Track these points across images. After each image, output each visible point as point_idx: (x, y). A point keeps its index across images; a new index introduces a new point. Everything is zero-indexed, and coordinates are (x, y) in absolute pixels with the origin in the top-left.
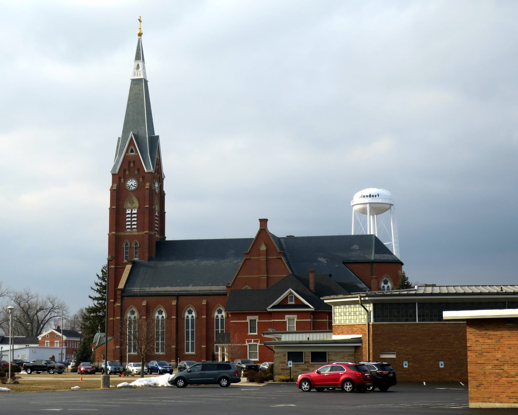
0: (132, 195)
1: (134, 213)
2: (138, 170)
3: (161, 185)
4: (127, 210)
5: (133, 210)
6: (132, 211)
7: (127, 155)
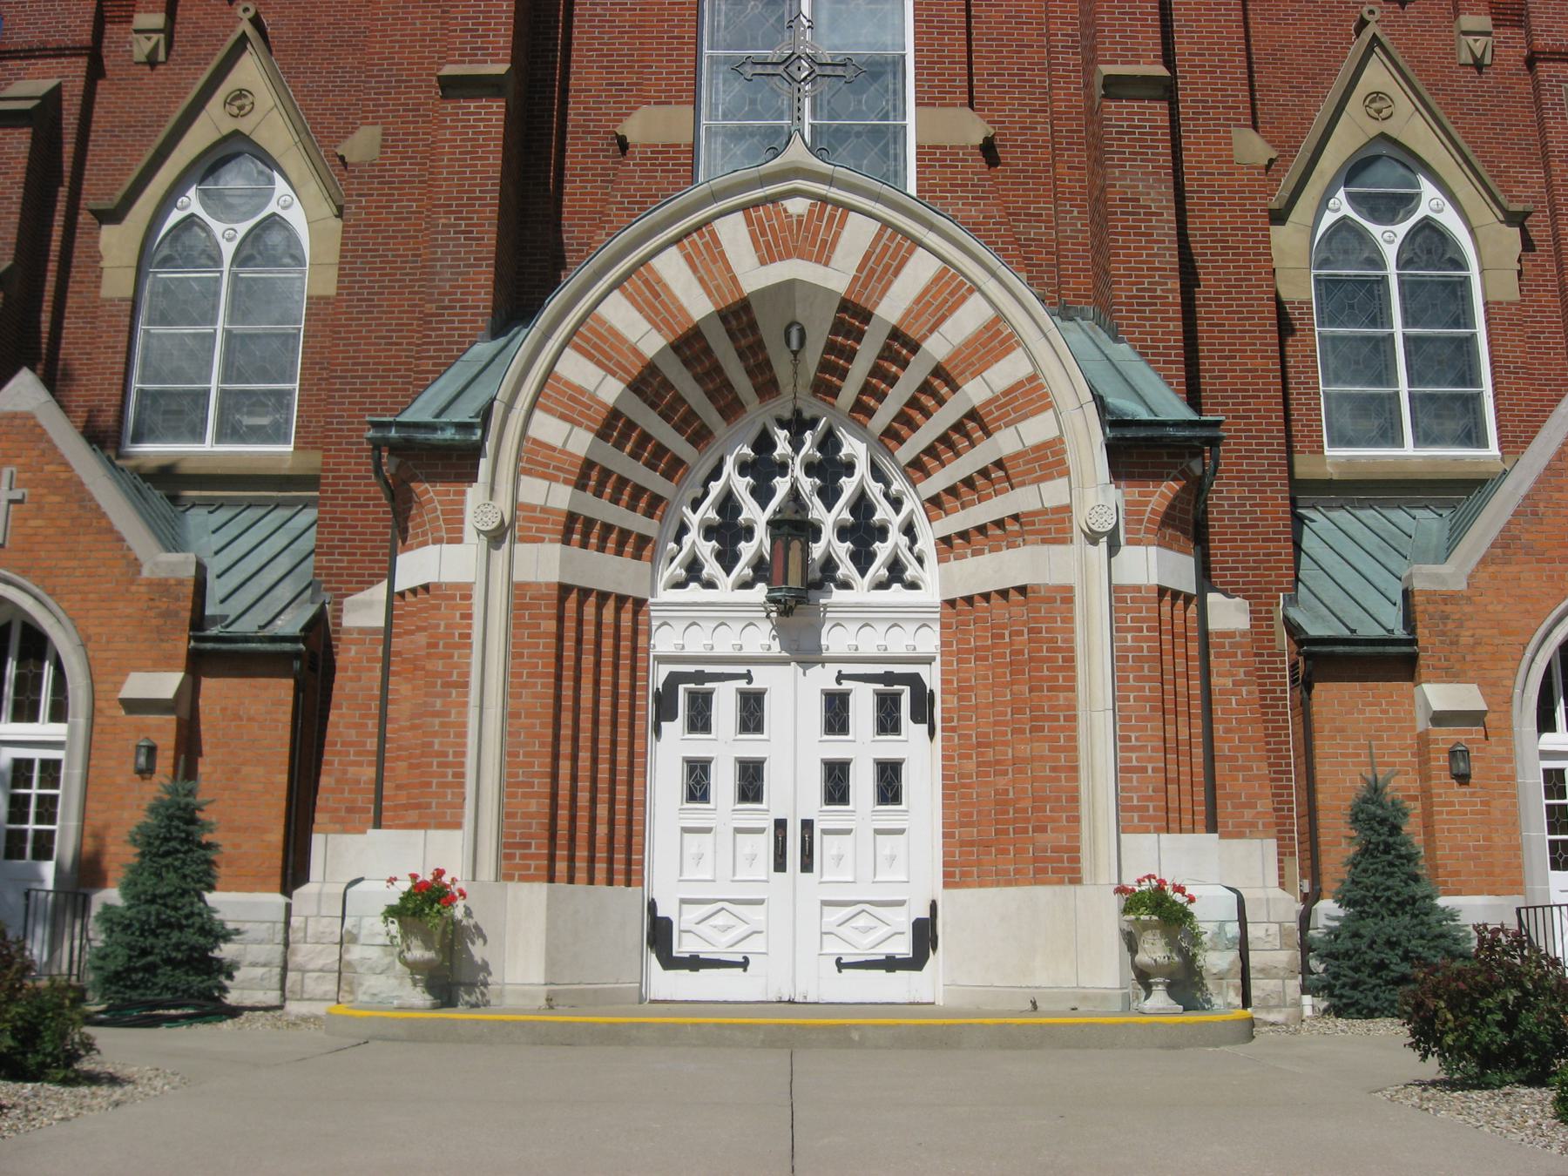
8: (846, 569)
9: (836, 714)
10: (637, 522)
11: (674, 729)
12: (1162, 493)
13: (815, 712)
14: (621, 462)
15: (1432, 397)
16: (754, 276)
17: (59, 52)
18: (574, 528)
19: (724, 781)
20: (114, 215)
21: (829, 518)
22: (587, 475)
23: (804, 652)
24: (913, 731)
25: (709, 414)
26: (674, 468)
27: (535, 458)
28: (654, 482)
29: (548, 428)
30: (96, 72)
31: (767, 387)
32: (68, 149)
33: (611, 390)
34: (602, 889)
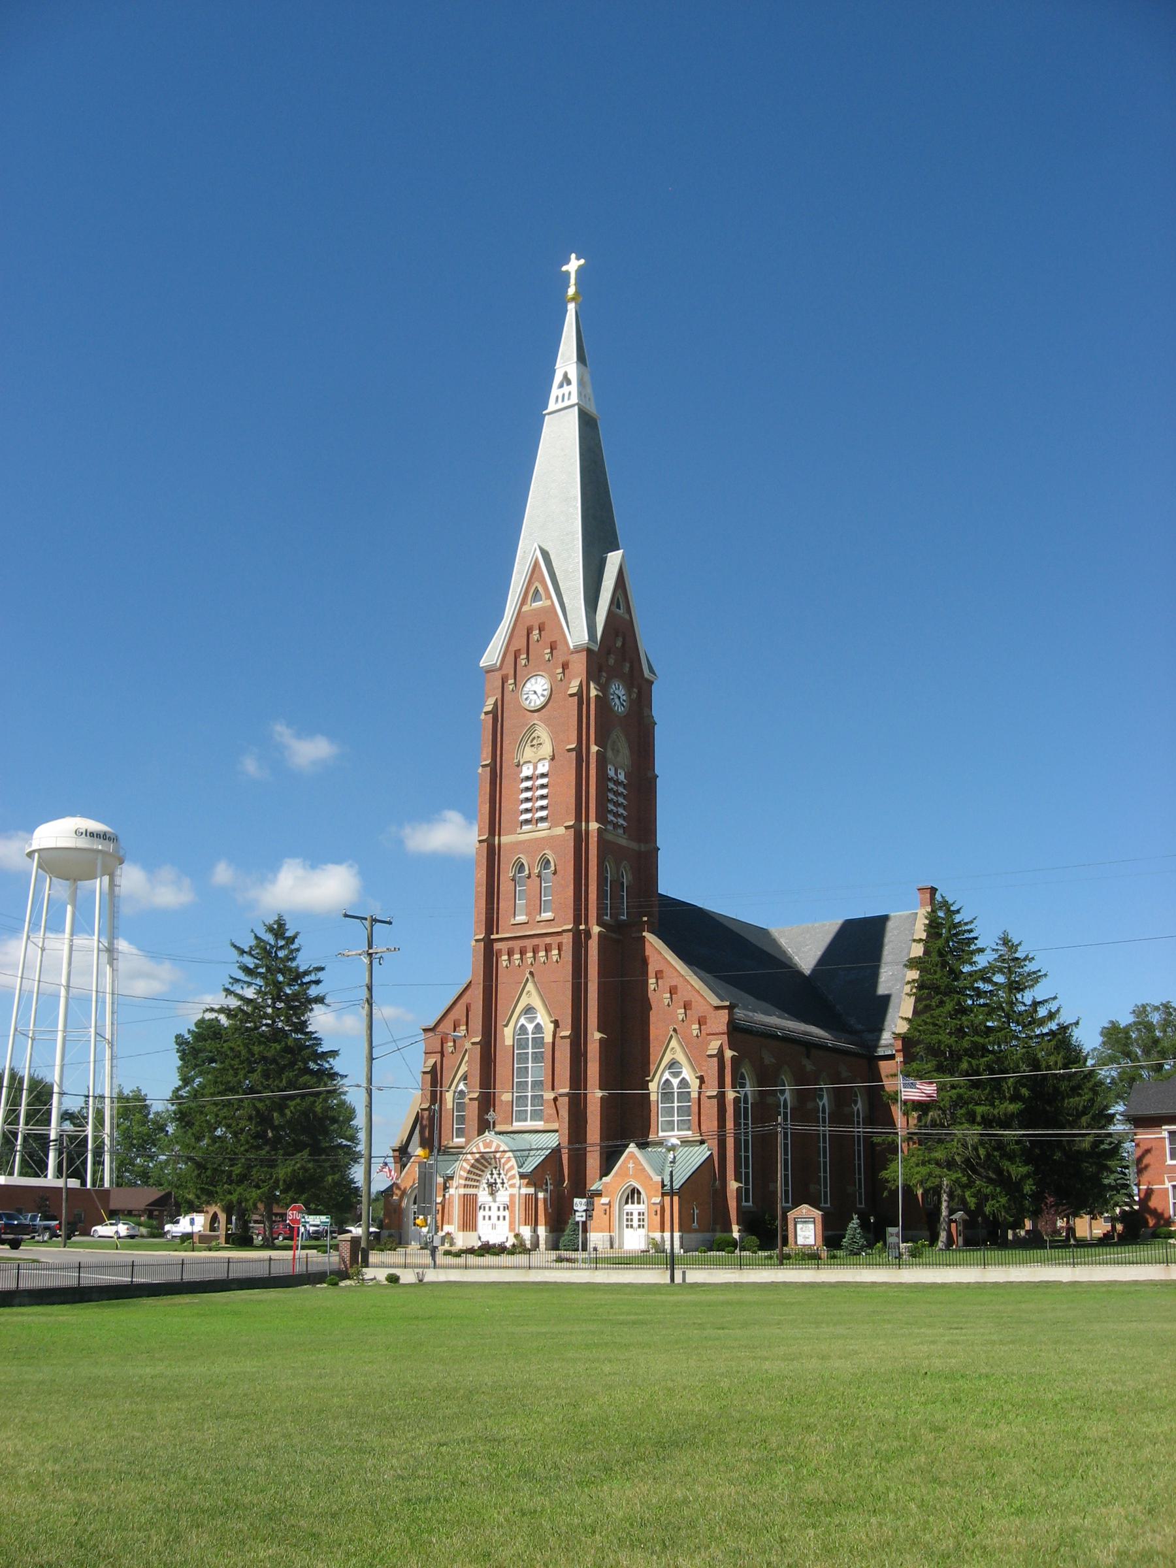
0: (536, 722)
1: (543, 776)
2: (553, 647)
3: (639, 693)
4: (524, 768)
5: (540, 765)
6: (535, 768)
7: (525, 609)
8: (501, 1188)
10: (475, 1184)
11: (482, 1211)
12: (526, 1181)
13: (496, 1209)
15: (682, 1120)
16: (483, 1150)
17: (435, 1053)
18: (465, 1186)
19: (487, 1218)
21: (499, 1181)
22: (466, 1179)
23: (495, 1201)
24: (507, 1211)
25: (483, 1168)
26: (480, 1176)
27: (461, 1177)
29: (462, 1173)
30: (442, 1055)
31: (490, 1164)
32: (439, 1075)
33: (468, 1168)
34: (471, 1232)
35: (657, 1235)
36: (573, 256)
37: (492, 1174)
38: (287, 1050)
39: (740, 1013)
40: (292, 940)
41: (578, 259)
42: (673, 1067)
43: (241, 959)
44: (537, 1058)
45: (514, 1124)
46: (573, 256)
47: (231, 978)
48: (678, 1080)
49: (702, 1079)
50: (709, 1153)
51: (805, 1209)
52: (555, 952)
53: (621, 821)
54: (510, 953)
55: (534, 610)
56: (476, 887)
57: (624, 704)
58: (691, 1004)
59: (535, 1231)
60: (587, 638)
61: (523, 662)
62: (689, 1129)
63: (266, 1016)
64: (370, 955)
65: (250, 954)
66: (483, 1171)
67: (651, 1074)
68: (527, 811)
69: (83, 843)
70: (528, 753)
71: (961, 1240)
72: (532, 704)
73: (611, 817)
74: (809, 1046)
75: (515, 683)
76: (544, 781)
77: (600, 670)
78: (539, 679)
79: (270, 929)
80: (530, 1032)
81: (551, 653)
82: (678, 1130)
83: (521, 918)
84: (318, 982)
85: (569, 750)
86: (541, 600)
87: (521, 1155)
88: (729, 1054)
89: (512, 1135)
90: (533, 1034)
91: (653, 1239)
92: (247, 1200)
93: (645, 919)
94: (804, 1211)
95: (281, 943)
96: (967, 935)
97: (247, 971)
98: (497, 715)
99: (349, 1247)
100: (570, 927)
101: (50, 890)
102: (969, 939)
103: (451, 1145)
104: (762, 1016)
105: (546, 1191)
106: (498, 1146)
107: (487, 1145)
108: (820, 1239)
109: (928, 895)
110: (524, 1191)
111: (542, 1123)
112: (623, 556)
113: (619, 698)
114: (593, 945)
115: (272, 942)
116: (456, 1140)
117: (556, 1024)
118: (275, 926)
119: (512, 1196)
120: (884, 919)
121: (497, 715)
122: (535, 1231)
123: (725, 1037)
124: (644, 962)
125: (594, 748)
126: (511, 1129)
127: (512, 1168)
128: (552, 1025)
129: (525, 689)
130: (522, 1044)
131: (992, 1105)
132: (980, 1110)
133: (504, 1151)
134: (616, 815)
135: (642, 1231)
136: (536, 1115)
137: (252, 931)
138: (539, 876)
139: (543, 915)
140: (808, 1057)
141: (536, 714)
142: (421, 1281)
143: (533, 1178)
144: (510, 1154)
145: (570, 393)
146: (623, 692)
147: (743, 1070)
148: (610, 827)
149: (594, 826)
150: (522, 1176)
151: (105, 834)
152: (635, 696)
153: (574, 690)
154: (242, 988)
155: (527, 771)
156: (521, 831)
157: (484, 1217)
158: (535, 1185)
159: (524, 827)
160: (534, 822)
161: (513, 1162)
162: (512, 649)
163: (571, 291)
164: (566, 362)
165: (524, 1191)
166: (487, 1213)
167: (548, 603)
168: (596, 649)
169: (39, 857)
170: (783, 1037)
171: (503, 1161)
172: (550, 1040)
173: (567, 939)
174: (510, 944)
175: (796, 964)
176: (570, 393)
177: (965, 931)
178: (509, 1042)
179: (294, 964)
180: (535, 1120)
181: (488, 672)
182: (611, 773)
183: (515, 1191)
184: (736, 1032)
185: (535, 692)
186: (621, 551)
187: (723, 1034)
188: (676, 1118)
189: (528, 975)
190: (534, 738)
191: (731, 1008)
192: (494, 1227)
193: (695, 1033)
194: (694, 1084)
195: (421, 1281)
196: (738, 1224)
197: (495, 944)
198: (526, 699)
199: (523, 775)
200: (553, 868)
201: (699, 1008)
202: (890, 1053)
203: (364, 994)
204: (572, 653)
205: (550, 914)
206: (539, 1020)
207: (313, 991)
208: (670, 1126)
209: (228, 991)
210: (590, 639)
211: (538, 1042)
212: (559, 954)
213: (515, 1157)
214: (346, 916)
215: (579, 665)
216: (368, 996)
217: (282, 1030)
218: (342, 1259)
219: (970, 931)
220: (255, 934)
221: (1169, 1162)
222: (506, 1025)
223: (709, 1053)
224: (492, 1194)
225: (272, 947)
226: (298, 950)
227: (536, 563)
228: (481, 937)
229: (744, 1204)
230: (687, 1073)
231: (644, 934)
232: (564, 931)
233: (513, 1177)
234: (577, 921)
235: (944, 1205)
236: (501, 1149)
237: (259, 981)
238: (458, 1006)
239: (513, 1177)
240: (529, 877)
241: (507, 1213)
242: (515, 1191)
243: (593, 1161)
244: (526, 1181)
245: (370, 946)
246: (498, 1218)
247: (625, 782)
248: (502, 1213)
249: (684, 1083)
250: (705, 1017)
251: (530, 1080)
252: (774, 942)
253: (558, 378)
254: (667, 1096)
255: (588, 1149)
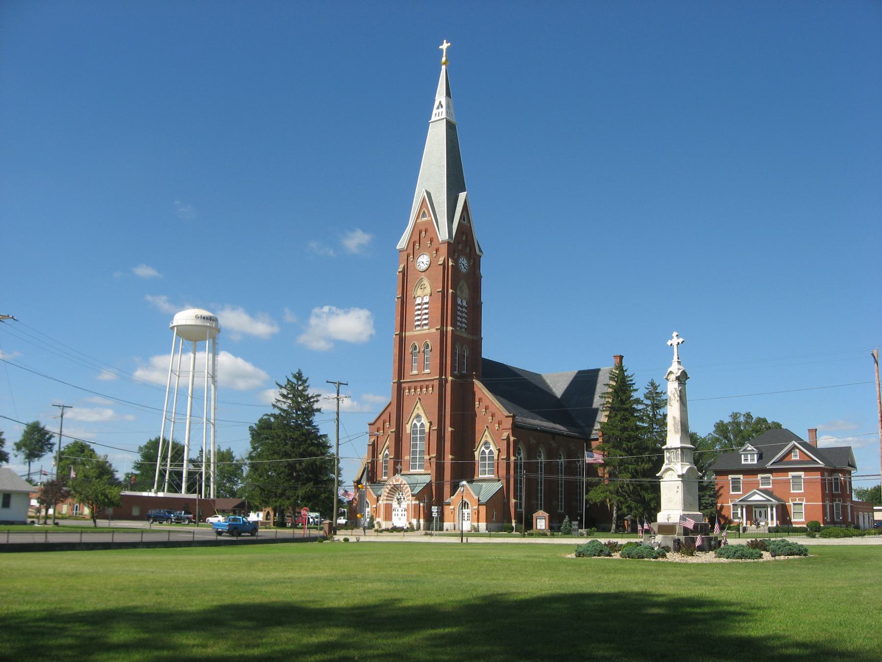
0: (423, 277)
1: (426, 303)
3: (474, 263)
4: (417, 299)
5: (425, 298)
6: (423, 300)
9: (402, 511)
12: (415, 498)
14: (390, 495)
16: (395, 483)
18: (387, 500)
19: (396, 515)
20: (380, 454)
21: (402, 498)
22: (387, 496)
26: (393, 495)
28: (392, 496)
31: (398, 490)
33: (388, 491)
35: (475, 524)
36: (445, 41)
37: (399, 494)
38: (303, 434)
39: (519, 419)
40: (305, 381)
41: (447, 43)
42: (487, 444)
43: (280, 391)
44: (421, 439)
45: (411, 470)
46: (445, 41)
47: (276, 399)
48: (488, 451)
49: (499, 450)
50: (502, 485)
51: (541, 513)
52: (431, 389)
53: (464, 325)
54: (409, 389)
55: (424, 222)
56: (394, 357)
57: (466, 268)
58: (495, 415)
59: (419, 521)
60: (448, 237)
61: (417, 247)
62: (493, 474)
63: (293, 418)
64: (338, 399)
65: (285, 388)
66: (395, 493)
67: (476, 447)
68: (418, 320)
69: (199, 322)
70: (419, 292)
71: (629, 529)
72: (421, 268)
73: (459, 324)
74: (554, 434)
75: (413, 257)
76: (427, 306)
77: (454, 252)
78: (425, 256)
79: (295, 376)
80: (418, 426)
81: (431, 243)
82: (488, 474)
83: (415, 372)
84: (317, 401)
85: (438, 292)
86: (426, 217)
87: (413, 486)
88: (512, 439)
89: (409, 476)
90: (420, 427)
91: (473, 526)
92: (284, 506)
93: (474, 373)
94: (541, 514)
95: (300, 383)
96: (629, 383)
97: (284, 396)
98: (404, 273)
99: (328, 526)
100: (438, 377)
101: (182, 345)
102: (630, 384)
103: (381, 480)
104: (531, 420)
105: (424, 502)
106: (402, 481)
107: (397, 481)
108: (547, 527)
109: (619, 360)
110: (414, 502)
111: (423, 470)
112: (467, 195)
113: (464, 265)
114: (449, 386)
115: (296, 383)
116: (384, 477)
117: (431, 423)
118: (297, 375)
119: (408, 505)
120: (598, 370)
121: (404, 273)
122: (419, 521)
123: (511, 430)
124: (474, 394)
125: (450, 291)
126: (409, 473)
127: (408, 492)
128: (429, 424)
129: (418, 261)
130: (415, 432)
131: (638, 465)
132: (630, 467)
133: (405, 484)
134: (462, 322)
135: (469, 522)
136: (421, 467)
137: (286, 377)
138: (424, 352)
139: (425, 371)
140: (554, 440)
141: (423, 273)
142: (358, 541)
143: (418, 497)
144: (408, 486)
145: (442, 112)
146: (466, 262)
147: (520, 446)
148: (458, 328)
149: (450, 328)
150: (413, 495)
151: (211, 317)
152: (471, 264)
153: (441, 262)
154: (281, 404)
155: (418, 301)
156: (416, 330)
157: (395, 515)
158: (419, 500)
159: (417, 328)
160: (422, 325)
161: (409, 489)
162: (412, 241)
163: (444, 59)
164: (441, 97)
165: (414, 502)
166: (396, 513)
167: (430, 218)
168: (452, 242)
169: (177, 330)
170: (540, 430)
171: (404, 488)
172: (428, 431)
173: (436, 383)
174: (410, 384)
175: (553, 393)
176: (442, 112)
177: (629, 380)
178: (408, 431)
179: (306, 393)
180: (420, 469)
181: (400, 252)
182: (459, 302)
183: (409, 502)
184: (516, 428)
185: (423, 263)
186: (466, 192)
187: (510, 429)
188: (487, 469)
189: (418, 400)
190: (422, 285)
191: (514, 417)
192: (400, 519)
193: (496, 428)
194: (496, 453)
195: (358, 541)
196: (515, 519)
197: (402, 384)
198: (419, 266)
199: (417, 303)
200: (430, 348)
201: (499, 417)
202: (596, 437)
203: (335, 416)
204: (441, 244)
205: (428, 370)
206: (423, 421)
207: (316, 406)
208: (484, 472)
209: (274, 406)
210: (449, 238)
211: (422, 432)
212: (433, 390)
213: (410, 487)
214: (327, 382)
215: (444, 250)
216: (337, 417)
217: (300, 424)
218: (325, 532)
219: (631, 380)
220: (288, 380)
221: (731, 493)
222: (407, 424)
223: (502, 438)
224: (399, 503)
225: (296, 385)
226: (308, 386)
227: (424, 199)
228: (396, 381)
229: (518, 510)
230: (492, 448)
231: (474, 380)
232: (435, 379)
233: (409, 496)
234: (441, 374)
235: (615, 512)
236: (403, 483)
237: (289, 401)
238: (386, 412)
239: (409, 496)
240: (419, 352)
241: (406, 513)
242: (409, 502)
243: (447, 489)
244: (415, 498)
245: (338, 395)
246: (402, 515)
247: (466, 306)
248: (403, 513)
249: (491, 452)
250: (501, 421)
251: (418, 450)
252: (543, 381)
253: (436, 104)
254: (483, 459)
255: (445, 483)
